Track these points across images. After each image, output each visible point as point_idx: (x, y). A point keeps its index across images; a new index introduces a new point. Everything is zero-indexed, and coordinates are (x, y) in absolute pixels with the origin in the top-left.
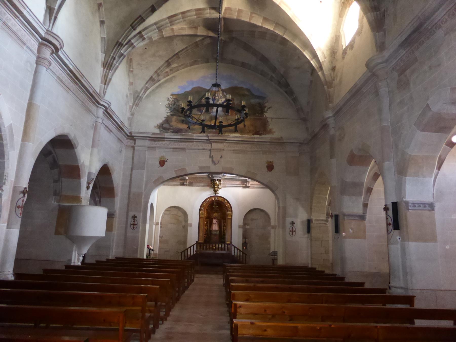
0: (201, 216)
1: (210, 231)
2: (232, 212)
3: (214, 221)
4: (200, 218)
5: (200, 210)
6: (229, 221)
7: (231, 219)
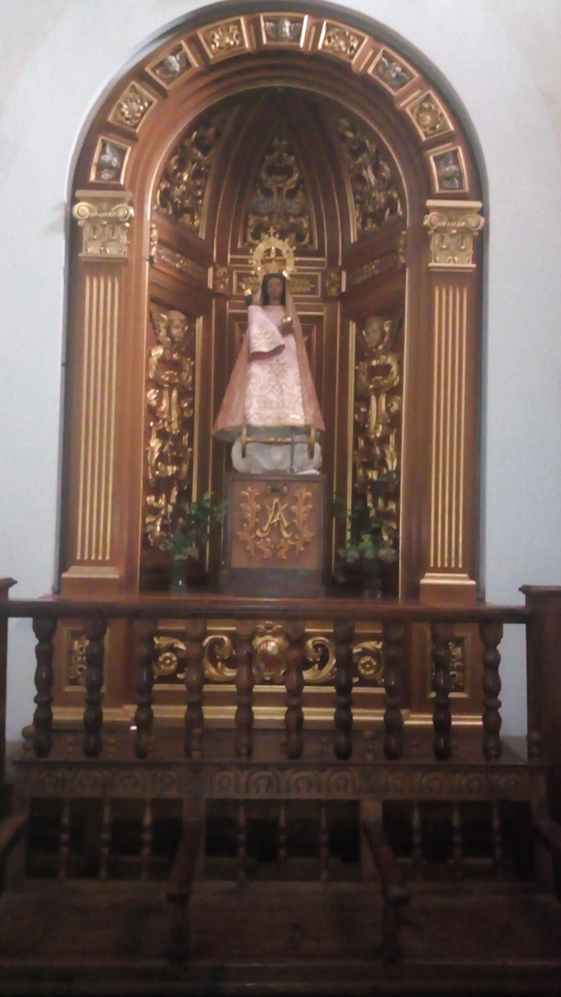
0: (91, 249)
1: (219, 450)
2: (479, 190)
3: (263, 327)
4: (76, 270)
5: (79, 180)
6: (449, 306)
7: (475, 283)
